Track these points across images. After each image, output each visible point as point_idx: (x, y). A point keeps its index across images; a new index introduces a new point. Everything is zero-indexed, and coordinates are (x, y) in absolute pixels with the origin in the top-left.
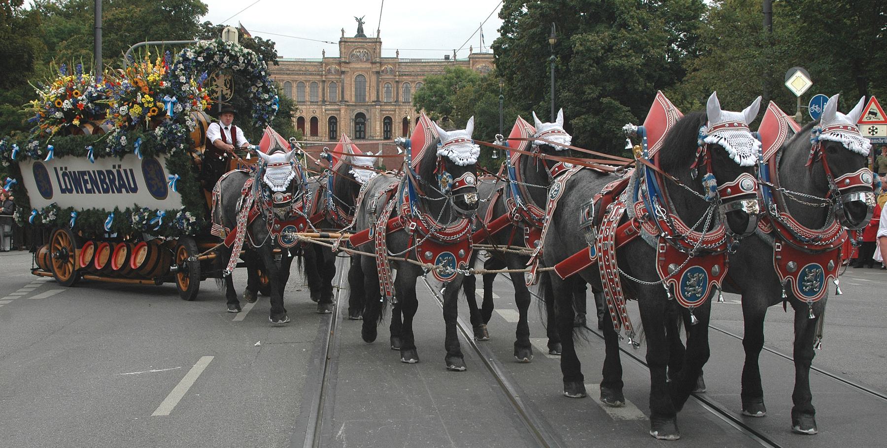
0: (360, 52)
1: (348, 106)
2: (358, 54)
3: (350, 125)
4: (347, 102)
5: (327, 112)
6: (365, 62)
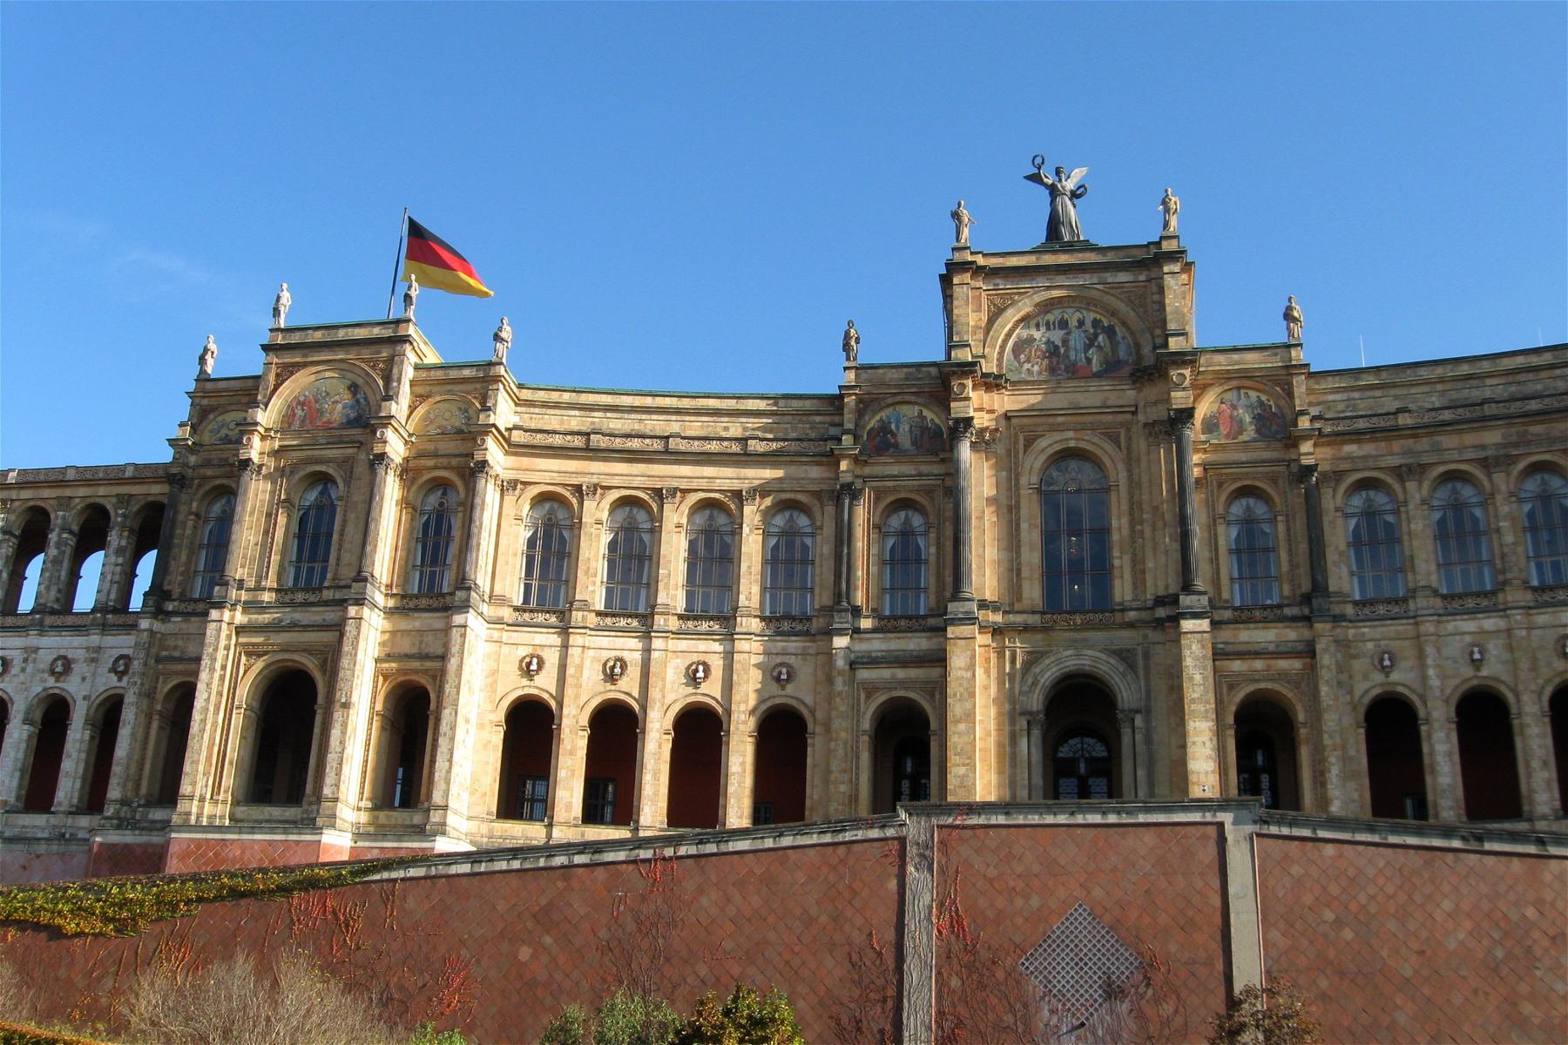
0: (1063, 324)
5: (864, 674)
6: (1097, 375)
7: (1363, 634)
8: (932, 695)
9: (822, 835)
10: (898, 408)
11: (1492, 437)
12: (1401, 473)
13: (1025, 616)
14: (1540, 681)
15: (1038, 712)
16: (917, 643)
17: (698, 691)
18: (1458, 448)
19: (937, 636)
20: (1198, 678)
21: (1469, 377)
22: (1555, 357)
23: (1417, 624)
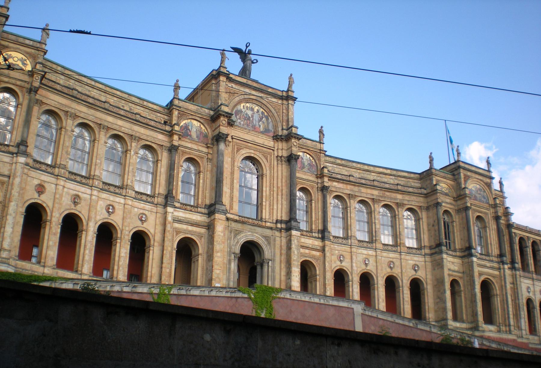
0: (252, 109)
2: (250, 113)
3: (230, 268)
5: (177, 225)
6: (262, 133)
7: (335, 248)
8: (201, 239)
9: (227, 293)
10: (192, 121)
11: (376, 192)
12: (350, 196)
13: (234, 215)
14: (383, 274)
15: (238, 254)
17: (109, 217)
18: (367, 193)
19: (204, 216)
20: (296, 252)
21: (367, 171)
22: (391, 172)
23: (351, 248)
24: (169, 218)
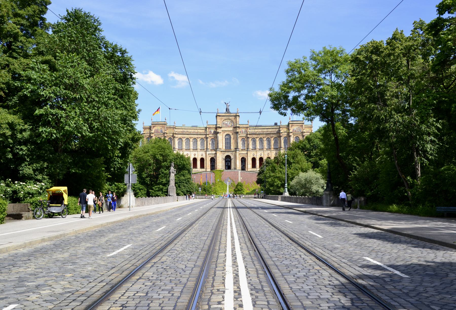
1: (221, 151)
2: (227, 122)
4: (221, 149)
16: (214, 152)
24: (207, 154)
